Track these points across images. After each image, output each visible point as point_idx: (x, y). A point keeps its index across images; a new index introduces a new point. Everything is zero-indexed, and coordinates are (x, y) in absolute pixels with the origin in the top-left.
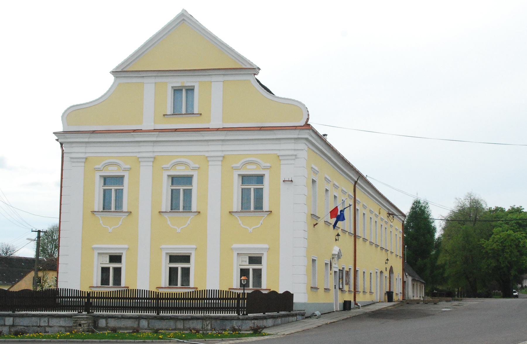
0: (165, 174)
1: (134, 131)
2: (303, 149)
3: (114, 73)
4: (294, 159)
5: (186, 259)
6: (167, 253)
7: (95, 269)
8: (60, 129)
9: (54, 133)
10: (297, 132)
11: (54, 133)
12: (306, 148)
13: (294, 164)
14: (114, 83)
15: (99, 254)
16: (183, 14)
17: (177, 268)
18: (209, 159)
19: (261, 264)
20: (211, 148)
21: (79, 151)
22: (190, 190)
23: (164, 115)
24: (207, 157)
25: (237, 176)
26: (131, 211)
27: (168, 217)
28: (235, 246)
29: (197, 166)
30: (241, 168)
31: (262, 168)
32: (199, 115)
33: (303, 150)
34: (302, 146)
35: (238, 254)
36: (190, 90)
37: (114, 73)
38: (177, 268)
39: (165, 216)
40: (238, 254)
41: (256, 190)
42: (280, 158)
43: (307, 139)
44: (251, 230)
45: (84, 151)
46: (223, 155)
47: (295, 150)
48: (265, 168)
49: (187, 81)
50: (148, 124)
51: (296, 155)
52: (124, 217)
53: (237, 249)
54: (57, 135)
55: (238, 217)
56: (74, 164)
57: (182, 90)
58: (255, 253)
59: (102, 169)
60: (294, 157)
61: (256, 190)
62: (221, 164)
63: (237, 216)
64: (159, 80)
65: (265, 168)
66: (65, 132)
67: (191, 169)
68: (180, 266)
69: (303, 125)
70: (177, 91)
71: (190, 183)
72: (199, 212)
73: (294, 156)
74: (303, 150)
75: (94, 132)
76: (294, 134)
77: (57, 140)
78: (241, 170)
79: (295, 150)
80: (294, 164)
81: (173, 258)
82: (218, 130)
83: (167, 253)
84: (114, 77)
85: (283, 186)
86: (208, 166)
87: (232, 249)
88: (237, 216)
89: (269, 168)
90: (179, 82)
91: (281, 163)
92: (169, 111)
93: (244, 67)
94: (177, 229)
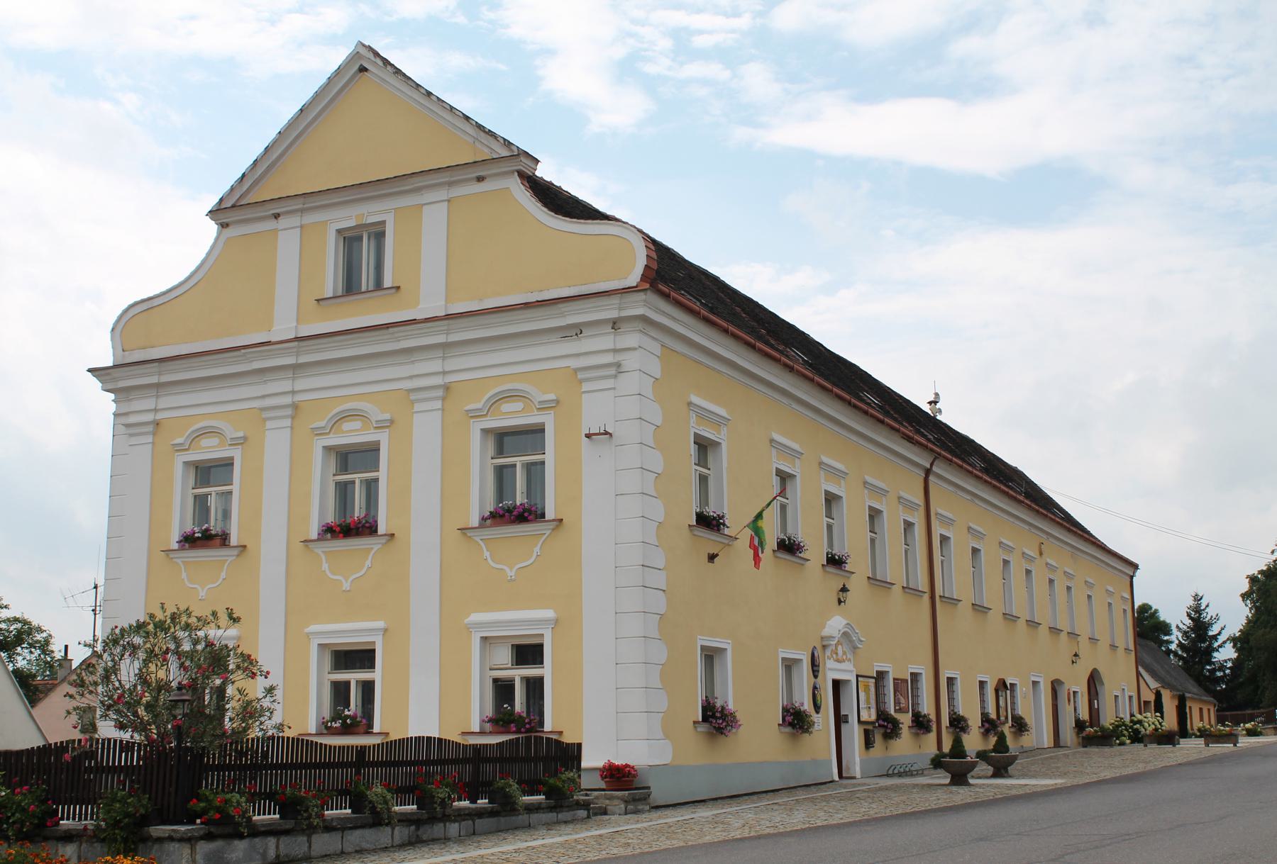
2: (637, 347)
3: (213, 213)
9: (89, 370)
10: (615, 300)
11: (89, 370)
12: (656, 348)
13: (614, 389)
14: (217, 239)
16: (358, 52)
17: (347, 684)
22: (376, 480)
25: (479, 432)
26: (245, 544)
28: (475, 617)
30: (488, 411)
31: (538, 407)
32: (394, 290)
33: (635, 349)
34: (631, 339)
35: (484, 639)
36: (379, 235)
37: (213, 213)
38: (347, 684)
39: (316, 550)
41: (529, 467)
43: (644, 319)
44: (513, 574)
47: (615, 351)
49: (369, 212)
50: (283, 328)
51: (618, 365)
52: (230, 559)
53: (481, 625)
54: (97, 373)
55: (480, 542)
56: (134, 440)
57: (360, 239)
58: (524, 633)
60: (612, 371)
61: (529, 467)
62: (440, 407)
64: (309, 219)
66: (115, 367)
67: (375, 426)
68: (354, 677)
69: (635, 285)
70: (350, 240)
72: (393, 535)
73: (615, 369)
74: (635, 349)
76: (608, 311)
79: (615, 351)
80: (614, 389)
84: (216, 226)
87: (469, 628)
88: (478, 539)
89: (554, 405)
90: (348, 217)
94: (343, 581)
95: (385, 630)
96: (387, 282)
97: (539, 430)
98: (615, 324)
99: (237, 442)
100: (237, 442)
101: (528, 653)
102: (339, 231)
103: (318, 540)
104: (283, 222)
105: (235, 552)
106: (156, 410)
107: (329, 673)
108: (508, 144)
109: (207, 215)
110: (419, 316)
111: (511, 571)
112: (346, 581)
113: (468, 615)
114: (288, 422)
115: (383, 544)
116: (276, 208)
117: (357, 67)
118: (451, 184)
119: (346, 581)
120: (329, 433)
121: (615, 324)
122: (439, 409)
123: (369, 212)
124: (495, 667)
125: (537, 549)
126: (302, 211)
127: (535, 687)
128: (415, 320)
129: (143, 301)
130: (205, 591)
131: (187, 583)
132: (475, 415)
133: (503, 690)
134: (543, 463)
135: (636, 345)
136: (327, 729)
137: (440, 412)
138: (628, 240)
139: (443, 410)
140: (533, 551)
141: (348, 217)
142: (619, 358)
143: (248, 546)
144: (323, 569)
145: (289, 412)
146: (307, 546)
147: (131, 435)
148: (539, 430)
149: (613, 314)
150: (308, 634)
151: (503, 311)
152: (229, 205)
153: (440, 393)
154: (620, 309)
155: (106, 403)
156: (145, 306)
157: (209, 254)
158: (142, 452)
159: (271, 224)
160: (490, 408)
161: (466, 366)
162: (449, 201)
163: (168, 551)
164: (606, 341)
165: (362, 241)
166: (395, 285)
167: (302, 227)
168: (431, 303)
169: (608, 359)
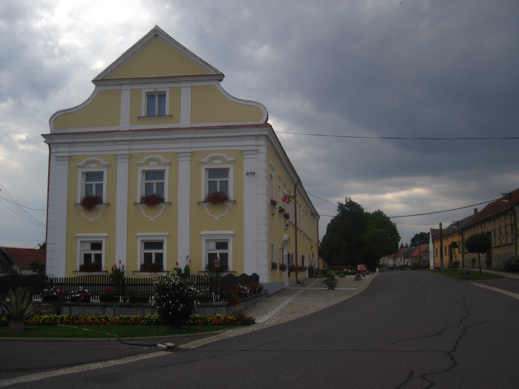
0: (140, 169)
1: (112, 132)
3: (94, 81)
4: (256, 154)
5: (159, 245)
6: (142, 241)
7: (78, 256)
8: (48, 132)
9: (42, 135)
10: (258, 129)
11: (42, 135)
14: (95, 91)
15: (81, 242)
16: (156, 29)
17: (151, 254)
18: (179, 155)
19: (227, 249)
20: (181, 145)
21: (63, 151)
23: (139, 117)
24: (177, 153)
25: (204, 170)
26: (109, 203)
27: (142, 208)
28: (203, 232)
29: (168, 161)
30: (208, 162)
31: (227, 162)
32: (170, 117)
35: (206, 240)
36: (162, 96)
37: (94, 81)
38: (151, 254)
40: (206, 240)
42: (243, 153)
45: (68, 150)
46: (191, 151)
47: (256, 145)
48: (230, 162)
49: (160, 88)
50: (125, 125)
51: (257, 150)
52: (103, 208)
54: (45, 136)
57: (154, 96)
59: (84, 166)
60: (255, 152)
62: (190, 159)
63: (204, 206)
64: (134, 87)
65: (230, 162)
67: (163, 164)
68: (154, 252)
69: (263, 124)
70: (150, 96)
71: (163, 178)
72: (171, 203)
73: (256, 151)
75: (76, 133)
76: (256, 132)
77: (45, 142)
78: (208, 165)
79: (256, 145)
81: (148, 245)
82: (187, 129)
83: (142, 241)
84: (95, 86)
85: (245, 177)
86: (178, 161)
87: (201, 235)
88: (204, 206)
89: (233, 162)
90: (151, 88)
91: (244, 158)
92: (143, 113)
93: (210, 74)
94: (151, 218)
95: (168, 236)
96: (167, 113)
97: (226, 170)
98: (257, 136)
99: (105, 166)
100: (105, 166)
101: (222, 245)
102: (146, 93)
103: (204, 202)
104: (123, 87)
105: (233, 203)
106: (70, 152)
107: (144, 250)
108: (216, 70)
109: (92, 81)
110: (181, 127)
111: (217, 218)
112: (152, 218)
113: (201, 232)
114: (127, 160)
115: (233, 204)
116: (120, 82)
117: (154, 34)
118: (192, 81)
119: (152, 218)
120: (144, 165)
121: (257, 136)
122: (189, 160)
123: (160, 88)
124: (210, 249)
125: (227, 211)
126: (132, 84)
127: (224, 257)
128: (179, 128)
129: (63, 111)
130: (92, 219)
131: (145, 215)
132: (204, 163)
133: (212, 257)
134: (227, 181)
135: (264, 144)
136: (145, 268)
137: (190, 161)
138: (259, 108)
139: (190, 161)
140: (225, 211)
141: (151, 88)
142: (257, 148)
143: (172, 203)
144: (143, 214)
145: (128, 157)
146: (200, 204)
147: (58, 160)
148: (226, 170)
149: (257, 133)
150: (137, 236)
151: (207, 129)
152: (100, 79)
153: (190, 155)
154: (259, 132)
155: (45, 149)
156: (64, 113)
157: (91, 96)
158: (63, 168)
159: (118, 88)
160: (209, 161)
161: (200, 146)
162: (191, 87)
163: (136, 204)
164: (253, 142)
165: (155, 97)
166: (171, 115)
167: (131, 90)
168: (185, 122)
169: (254, 148)
